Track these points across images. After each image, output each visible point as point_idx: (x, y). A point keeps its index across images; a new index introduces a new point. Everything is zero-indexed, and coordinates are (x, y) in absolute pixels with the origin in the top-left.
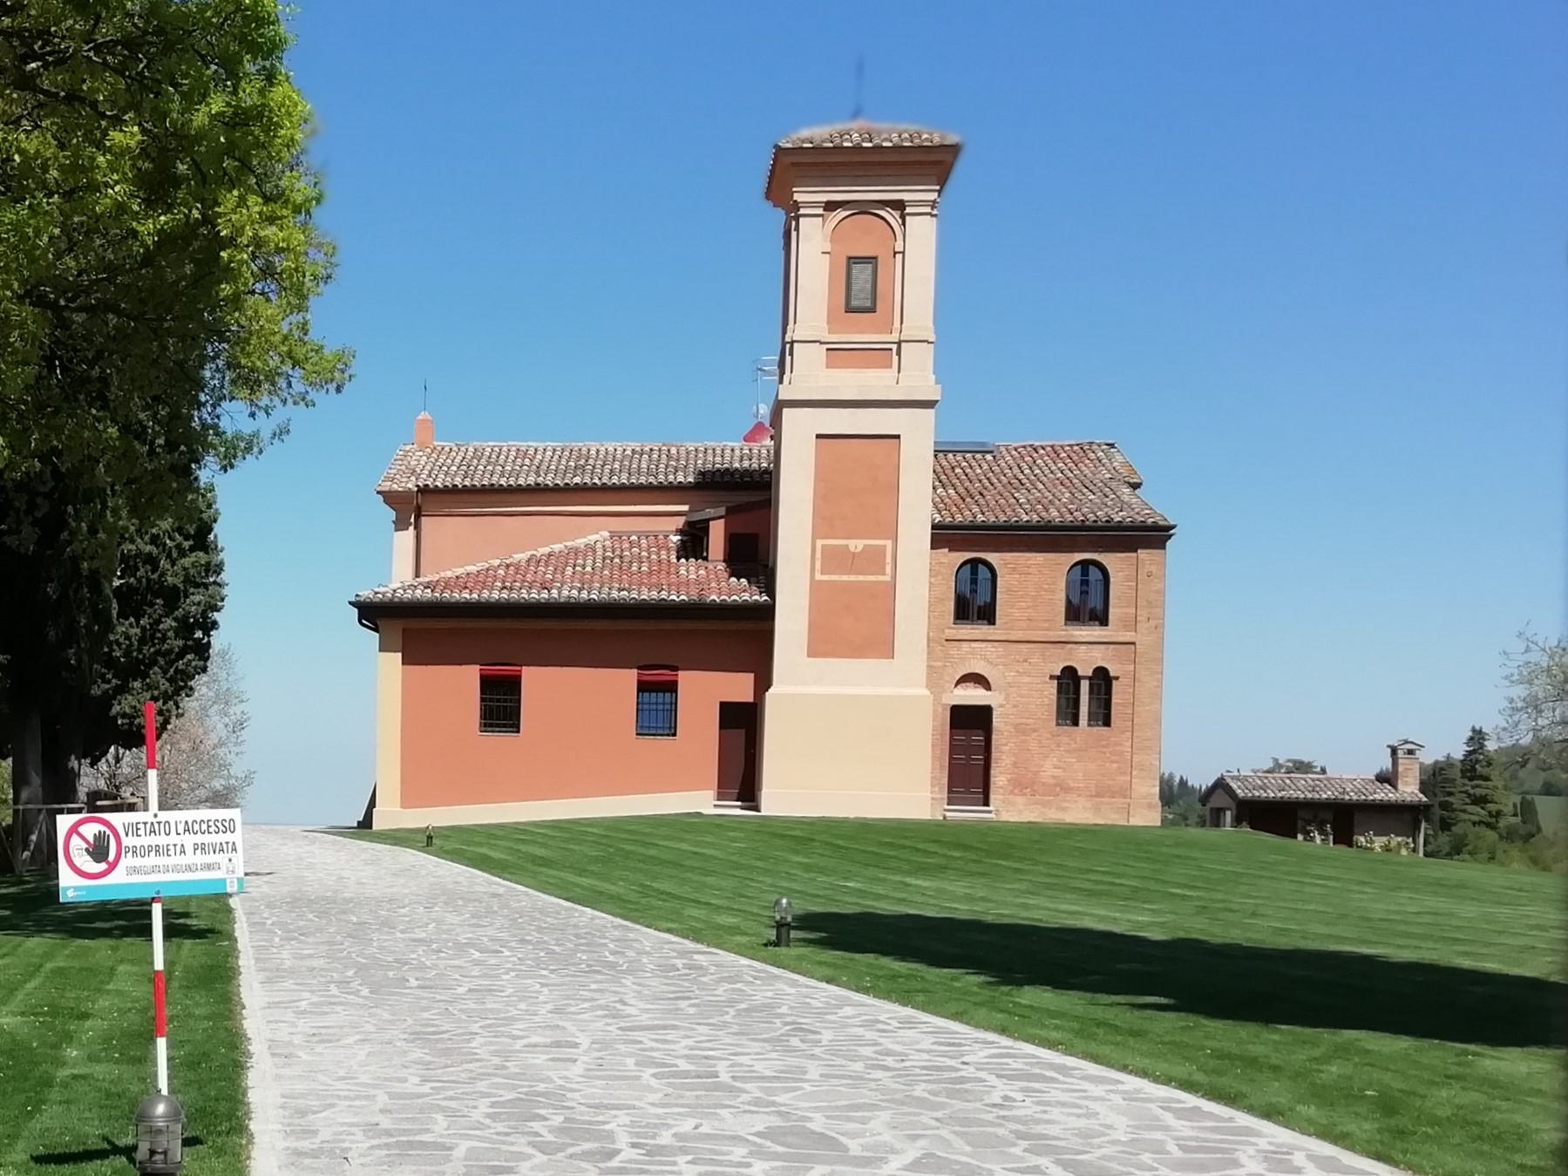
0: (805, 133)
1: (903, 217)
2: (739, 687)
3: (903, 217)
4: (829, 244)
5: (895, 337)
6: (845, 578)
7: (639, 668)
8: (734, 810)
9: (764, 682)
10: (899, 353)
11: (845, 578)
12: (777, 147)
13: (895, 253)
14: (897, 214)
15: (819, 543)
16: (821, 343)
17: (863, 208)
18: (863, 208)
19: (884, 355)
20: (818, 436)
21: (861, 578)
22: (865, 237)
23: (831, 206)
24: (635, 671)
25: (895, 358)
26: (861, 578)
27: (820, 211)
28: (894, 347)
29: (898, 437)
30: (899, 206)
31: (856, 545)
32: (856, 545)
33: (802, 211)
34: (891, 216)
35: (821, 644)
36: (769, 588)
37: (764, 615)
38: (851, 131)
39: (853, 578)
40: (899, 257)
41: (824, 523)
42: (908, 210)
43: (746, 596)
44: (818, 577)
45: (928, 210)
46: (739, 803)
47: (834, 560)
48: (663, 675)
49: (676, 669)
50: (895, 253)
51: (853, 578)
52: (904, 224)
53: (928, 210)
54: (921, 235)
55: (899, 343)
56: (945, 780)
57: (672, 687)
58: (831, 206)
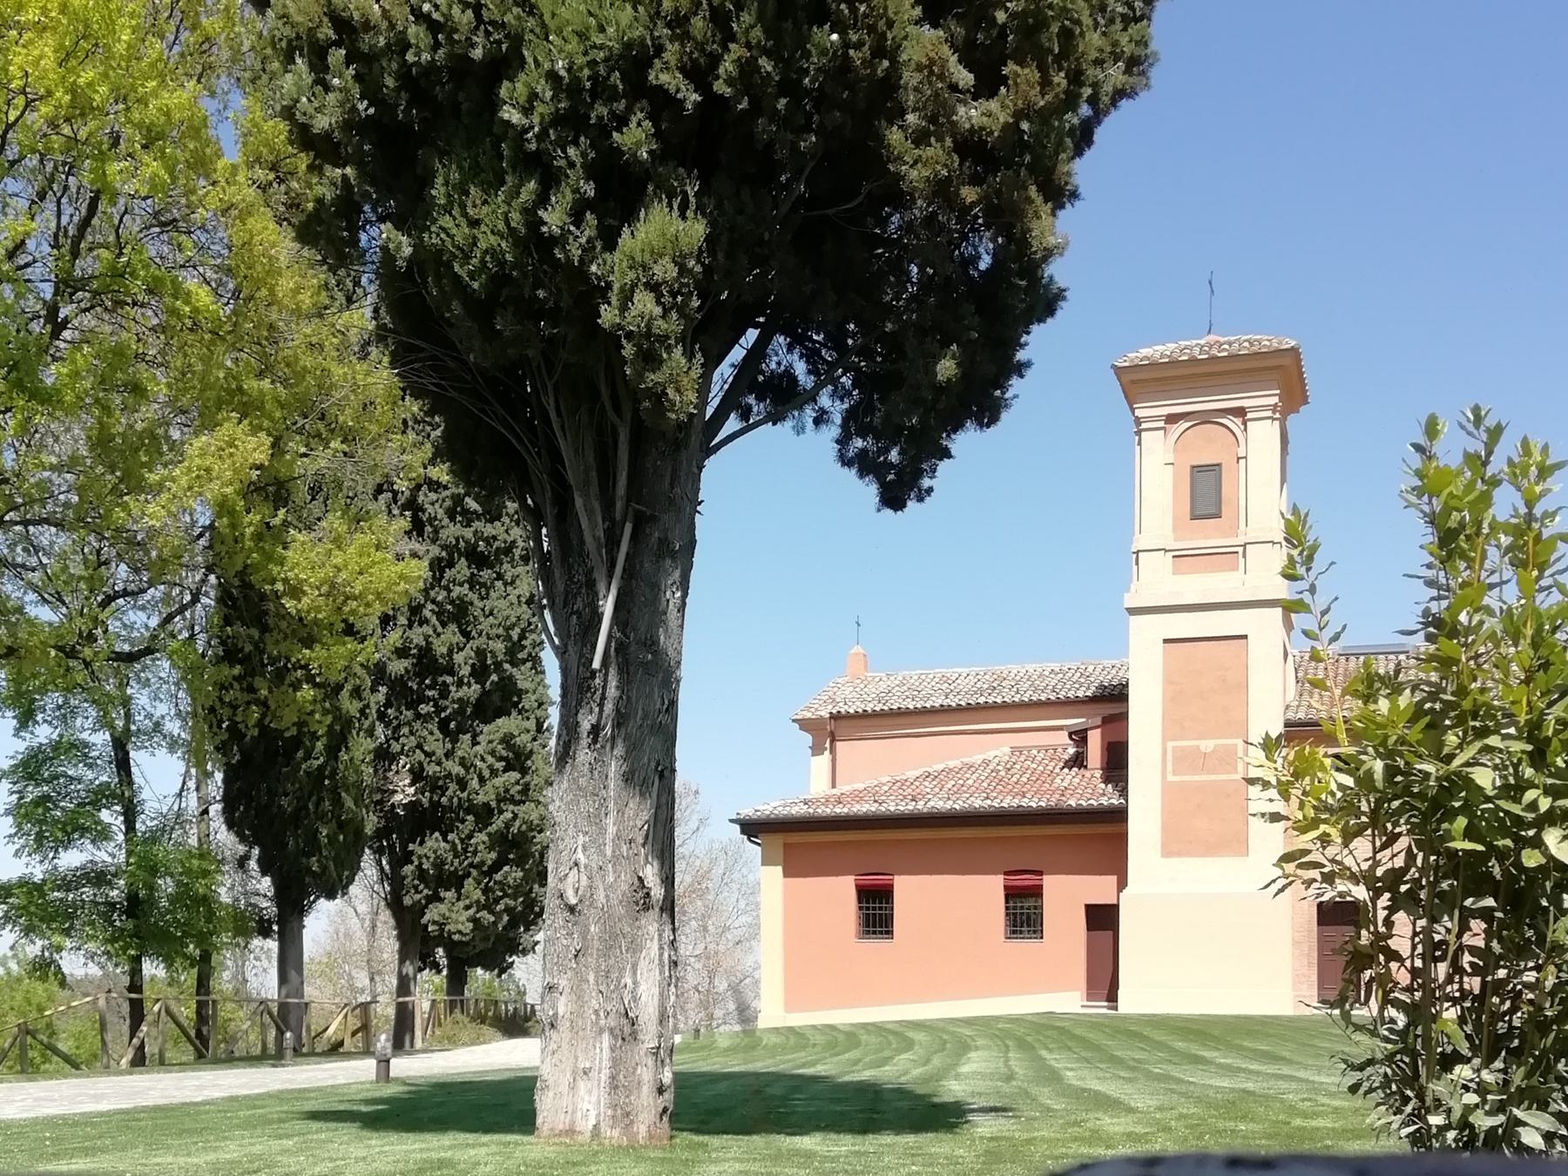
0: (1145, 352)
1: (1245, 423)
2: (1099, 889)
3: (1245, 423)
4: (1172, 455)
5: (1241, 540)
6: (1197, 778)
7: (1006, 873)
8: (1101, 1009)
9: (1122, 884)
10: (1244, 556)
11: (1197, 778)
12: (1118, 371)
13: (1239, 458)
14: (1238, 421)
15: (1170, 745)
16: (1166, 551)
17: (1205, 418)
18: (1205, 418)
19: (1230, 556)
20: (1166, 641)
21: (1213, 777)
22: (1207, 446)
23: (1172, 419)
24: (1001, 877)
25: (1242, 560)
26: (1213, 777)
27: (1162, 424)
28: (1240, 550)
29: (1245, 637)
30: (1240, 412)
31: (1207, 745)
32: (1207, 745)
33: (1144, 426)
34: (1234, 423)
35: (1175, 843)
36: (1124, 792)
37: (1118, 816)
38: (1194, 345)
39: (1205, 778)
40: (1242, 462)
41: (1173, 725)
42: (1249, 416)
43: (1104, 801)
44: (1171, 778)
45: (1269, 414)
46: (1106, 1004)
47: (1186, 760)
48: (1027, 880)
49: (1041, 873)
50: (1239, 458)
51: (1205, 778)
52: (1246, 430)
53: (1269, 414)
54: (1263, 437)
55: (1244, 546)
56: (1315, 978)
57: (1036, 892)
58: (1172, 419)
